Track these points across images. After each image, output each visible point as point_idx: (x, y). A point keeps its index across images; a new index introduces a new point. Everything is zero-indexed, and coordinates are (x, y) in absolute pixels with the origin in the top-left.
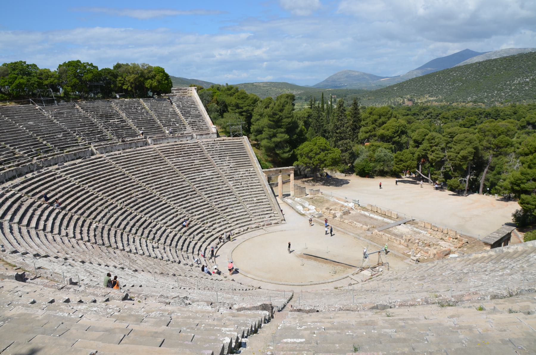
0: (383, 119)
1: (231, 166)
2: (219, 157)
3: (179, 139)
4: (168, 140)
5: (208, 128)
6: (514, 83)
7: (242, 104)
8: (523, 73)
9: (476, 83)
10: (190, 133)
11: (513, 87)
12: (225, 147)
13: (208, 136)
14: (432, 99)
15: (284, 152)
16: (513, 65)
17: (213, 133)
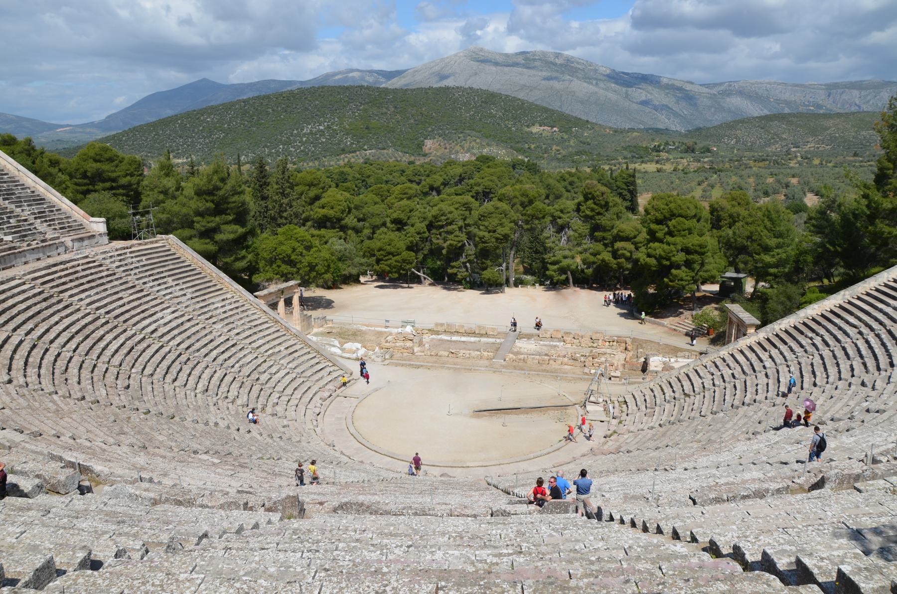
0: (313, 193)
1: (189, 296)
2: (153, 281)
3: (44, 254)
4: (25, 256)
5: (81, 225)
6: (304, 132)
7: (112, 172)
8: (313, 117)
9: (247, 133)
10: (58, 238)
11: (304, 139)
12: (147, 260)
13: (94, 241)
14: (180, 161)
15: (237, 259)
16: (294, 106)
17: (100, 235)
